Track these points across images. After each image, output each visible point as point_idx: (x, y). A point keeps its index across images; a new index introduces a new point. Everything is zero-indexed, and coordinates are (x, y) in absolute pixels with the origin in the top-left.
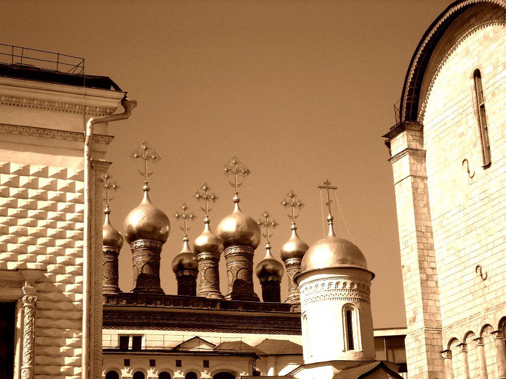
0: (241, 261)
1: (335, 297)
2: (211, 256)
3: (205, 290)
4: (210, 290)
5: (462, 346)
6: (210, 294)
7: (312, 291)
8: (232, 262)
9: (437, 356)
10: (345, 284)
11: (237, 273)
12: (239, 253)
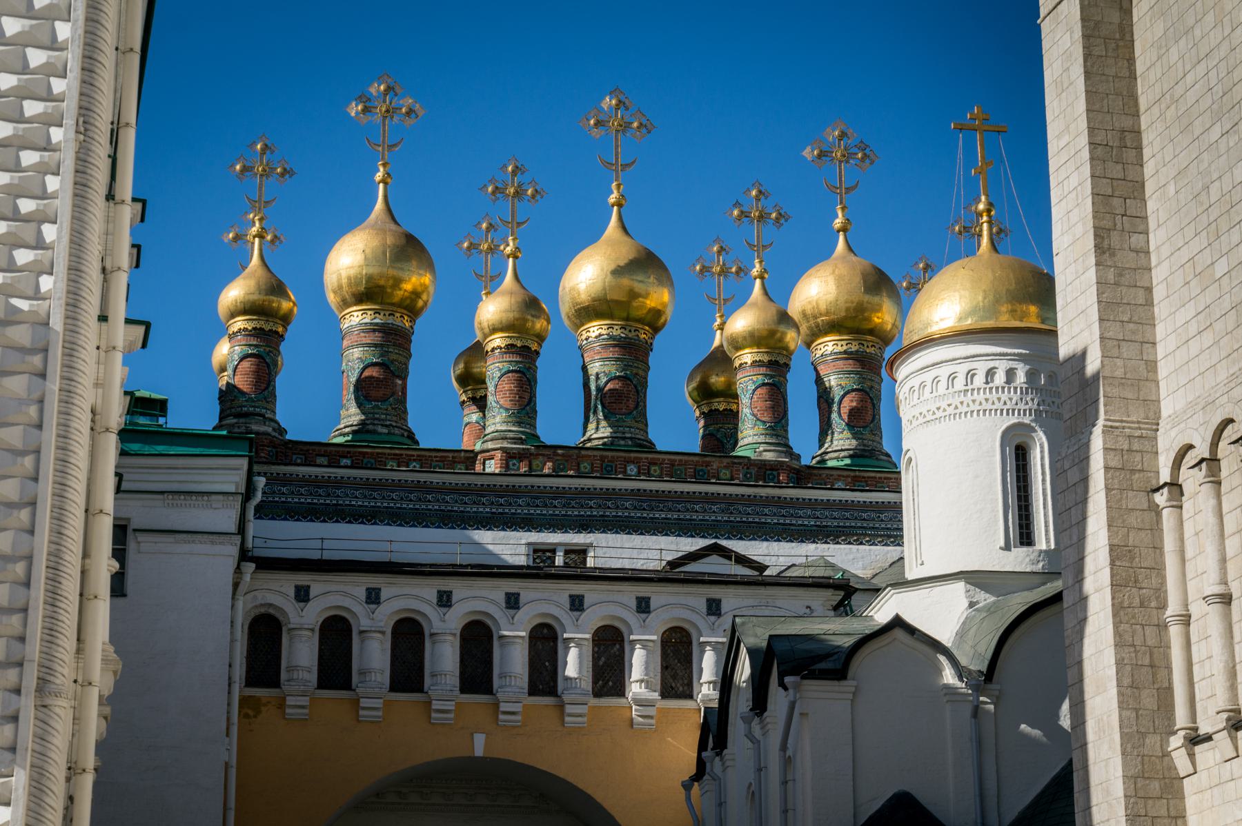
2: (765, 355)
5: (1204, 465)
6: (761, 449)
9: (1140, 501)
10: (1010, 374)
12: (845, 352)
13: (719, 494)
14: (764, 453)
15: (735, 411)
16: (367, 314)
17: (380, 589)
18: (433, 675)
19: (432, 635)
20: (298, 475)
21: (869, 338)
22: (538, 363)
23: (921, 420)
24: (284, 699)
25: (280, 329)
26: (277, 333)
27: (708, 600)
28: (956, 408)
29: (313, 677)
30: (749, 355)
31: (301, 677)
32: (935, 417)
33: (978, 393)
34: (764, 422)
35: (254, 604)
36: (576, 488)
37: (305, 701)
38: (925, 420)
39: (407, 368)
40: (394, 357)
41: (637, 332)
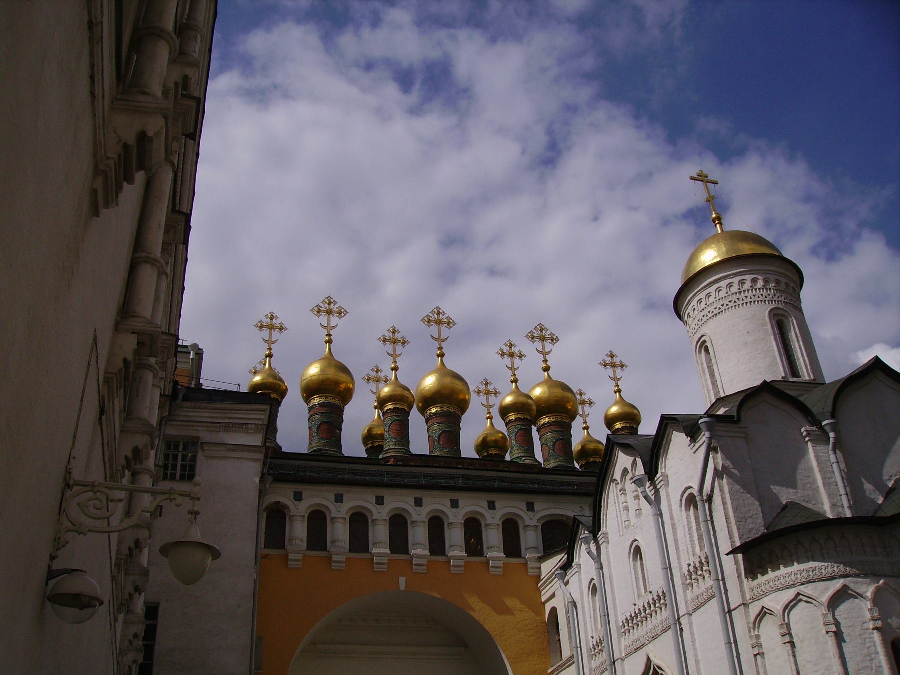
0: (555, 431)
1: (753, 300)
3: (517, 456)
4: (523, 455)
7: (712, 299)
8: (546, 433)
11: (554, 446)
14: (526, 461)
22: (409, 418)
23: (710, 315)
24: (287, 556)
25: (279, 399)
28: (735, 302)
30: (514, 416)
31: (297, 543)
32: (721, 310)
33: (748, 293)
34: (523, 447)
38: (713, 314)
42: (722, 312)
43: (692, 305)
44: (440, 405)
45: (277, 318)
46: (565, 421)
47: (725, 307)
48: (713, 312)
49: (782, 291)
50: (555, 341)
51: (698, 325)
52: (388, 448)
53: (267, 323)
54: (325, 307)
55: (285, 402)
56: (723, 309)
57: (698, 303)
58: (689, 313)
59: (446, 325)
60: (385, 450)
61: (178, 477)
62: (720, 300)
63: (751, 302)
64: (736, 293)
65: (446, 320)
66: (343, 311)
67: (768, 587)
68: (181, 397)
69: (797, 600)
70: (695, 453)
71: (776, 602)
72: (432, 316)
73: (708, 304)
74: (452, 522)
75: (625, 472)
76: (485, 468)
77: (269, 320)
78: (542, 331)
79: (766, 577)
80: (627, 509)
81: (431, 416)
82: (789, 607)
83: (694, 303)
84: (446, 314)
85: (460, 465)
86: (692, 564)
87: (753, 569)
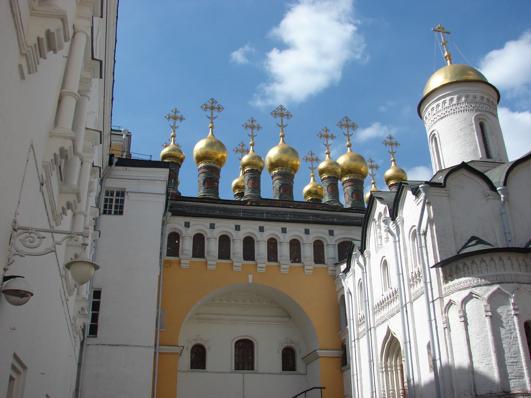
4: (332, 200)
7: (440, 108)
13: (320, 214)
15: (319, 199)
16: (206, 163)
17: (215, 224)
18: (234, 254)
19: (233, 240)
20: (184, 205)
21: (360, 175)
23: (438, 118)
26: (178, 164)
27: (329, 231)
28: (454, 110)
29: (191, 253)
31: (186, 253)
32: (445, 115)
34: (332, 195)
35: (170, 228)
36: (275, 211)
37: (188, 261)
38: (440, 117)
39: (219, 180)
40: (215, 176)
41: (290, 171)
42: (446, 116)
43: (428, 111)
44: (280, 168)
45: (179, 112)
46: (360, 179)
47: (448, 113)
48: (440, 116)
49: (484, 103)
50: (355, 128)
51: (431, 124)
52: (247, 194)
53: (173, 115)
54: (209, 105)
55: (183, 165)
56: (446, 114)
57: (431, 110)
58: (426, 116)
59: (286, 117)
60: (245, 196)
61: (113, 212)
62: (445, 108)
63: (464, 110)
64: (455, 104)
65: (286, 114)
66: (221, 107)
67: (454, 288)
68: (114, 164)
69: (470, 297)
70: (417, 205)
71: (458, 297)
72: (276, 110)
73: (438, 110)
74: (282, 241)
75: (380, 214)
76: (307, 208)
77: (174, 114)
78: (347, 122)
79: (454, 282)
80: (381, 237)
81: (275, 174)
82: (465, 301)
83: (429, 110)
84: (286, 110)
85: (292, 205)
86: (414, 273)
87: (448, 277)
